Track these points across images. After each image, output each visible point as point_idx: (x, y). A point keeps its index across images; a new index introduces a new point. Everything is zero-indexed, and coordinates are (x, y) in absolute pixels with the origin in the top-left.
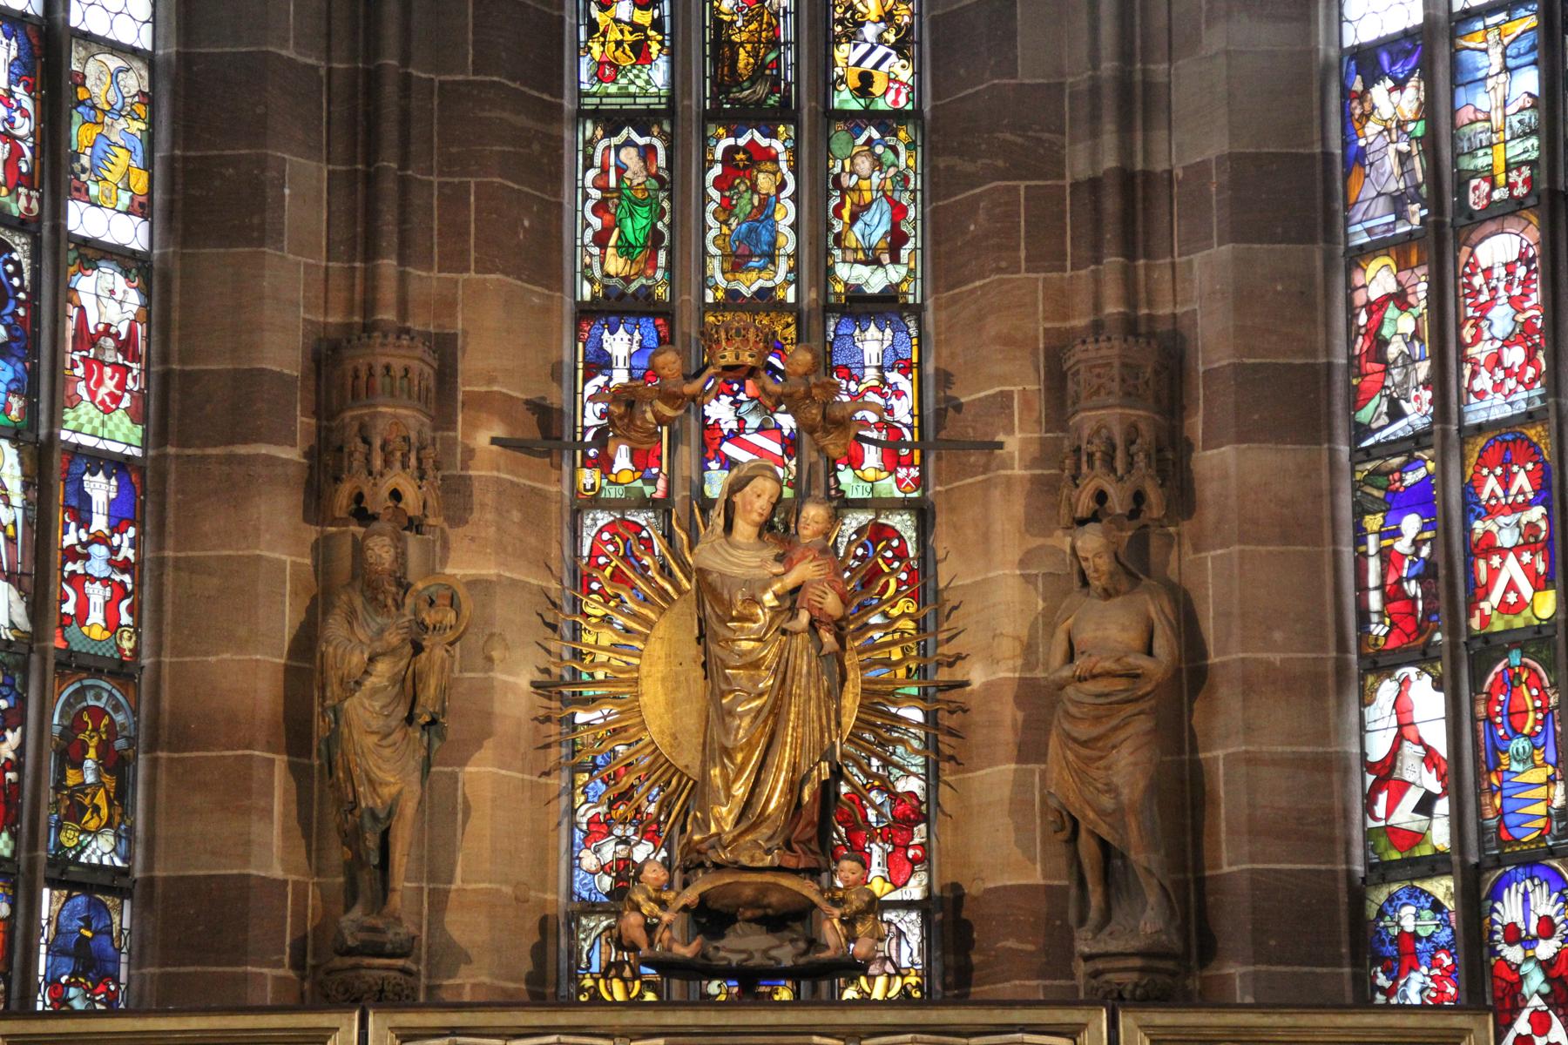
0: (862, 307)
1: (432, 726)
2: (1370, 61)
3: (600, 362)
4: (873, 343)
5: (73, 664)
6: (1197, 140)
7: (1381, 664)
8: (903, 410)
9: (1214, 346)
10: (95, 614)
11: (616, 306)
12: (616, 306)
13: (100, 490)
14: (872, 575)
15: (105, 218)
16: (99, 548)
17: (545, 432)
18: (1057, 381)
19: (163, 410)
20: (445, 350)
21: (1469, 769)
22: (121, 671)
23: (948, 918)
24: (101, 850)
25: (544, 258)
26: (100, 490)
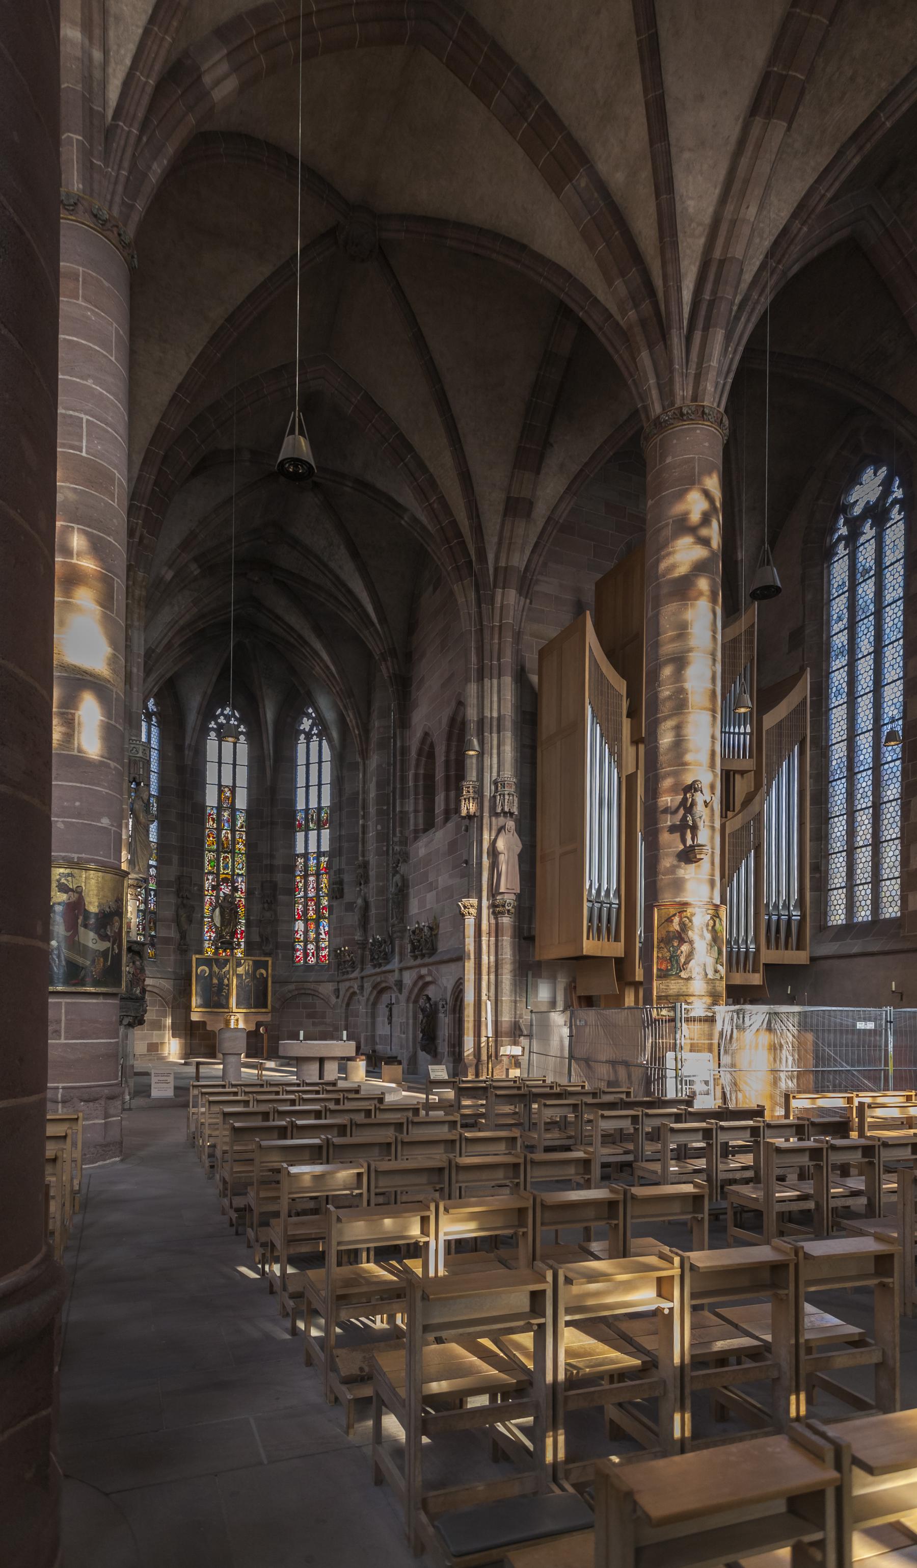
0: (238, 875)
1: (190, 920)
2: (298, 855)
3: (208, 879)
4: (240, 879)
5: (151, 912)
8: (243, 887)
11: (210, 873)
12: (210, 873)
13: (152, 893)
16: (152, 898)
18: (262, 886)
19: (158, 884)
20: (191, 878)
22: (155, 913)
24: (153, 933)
26: (152, 893)
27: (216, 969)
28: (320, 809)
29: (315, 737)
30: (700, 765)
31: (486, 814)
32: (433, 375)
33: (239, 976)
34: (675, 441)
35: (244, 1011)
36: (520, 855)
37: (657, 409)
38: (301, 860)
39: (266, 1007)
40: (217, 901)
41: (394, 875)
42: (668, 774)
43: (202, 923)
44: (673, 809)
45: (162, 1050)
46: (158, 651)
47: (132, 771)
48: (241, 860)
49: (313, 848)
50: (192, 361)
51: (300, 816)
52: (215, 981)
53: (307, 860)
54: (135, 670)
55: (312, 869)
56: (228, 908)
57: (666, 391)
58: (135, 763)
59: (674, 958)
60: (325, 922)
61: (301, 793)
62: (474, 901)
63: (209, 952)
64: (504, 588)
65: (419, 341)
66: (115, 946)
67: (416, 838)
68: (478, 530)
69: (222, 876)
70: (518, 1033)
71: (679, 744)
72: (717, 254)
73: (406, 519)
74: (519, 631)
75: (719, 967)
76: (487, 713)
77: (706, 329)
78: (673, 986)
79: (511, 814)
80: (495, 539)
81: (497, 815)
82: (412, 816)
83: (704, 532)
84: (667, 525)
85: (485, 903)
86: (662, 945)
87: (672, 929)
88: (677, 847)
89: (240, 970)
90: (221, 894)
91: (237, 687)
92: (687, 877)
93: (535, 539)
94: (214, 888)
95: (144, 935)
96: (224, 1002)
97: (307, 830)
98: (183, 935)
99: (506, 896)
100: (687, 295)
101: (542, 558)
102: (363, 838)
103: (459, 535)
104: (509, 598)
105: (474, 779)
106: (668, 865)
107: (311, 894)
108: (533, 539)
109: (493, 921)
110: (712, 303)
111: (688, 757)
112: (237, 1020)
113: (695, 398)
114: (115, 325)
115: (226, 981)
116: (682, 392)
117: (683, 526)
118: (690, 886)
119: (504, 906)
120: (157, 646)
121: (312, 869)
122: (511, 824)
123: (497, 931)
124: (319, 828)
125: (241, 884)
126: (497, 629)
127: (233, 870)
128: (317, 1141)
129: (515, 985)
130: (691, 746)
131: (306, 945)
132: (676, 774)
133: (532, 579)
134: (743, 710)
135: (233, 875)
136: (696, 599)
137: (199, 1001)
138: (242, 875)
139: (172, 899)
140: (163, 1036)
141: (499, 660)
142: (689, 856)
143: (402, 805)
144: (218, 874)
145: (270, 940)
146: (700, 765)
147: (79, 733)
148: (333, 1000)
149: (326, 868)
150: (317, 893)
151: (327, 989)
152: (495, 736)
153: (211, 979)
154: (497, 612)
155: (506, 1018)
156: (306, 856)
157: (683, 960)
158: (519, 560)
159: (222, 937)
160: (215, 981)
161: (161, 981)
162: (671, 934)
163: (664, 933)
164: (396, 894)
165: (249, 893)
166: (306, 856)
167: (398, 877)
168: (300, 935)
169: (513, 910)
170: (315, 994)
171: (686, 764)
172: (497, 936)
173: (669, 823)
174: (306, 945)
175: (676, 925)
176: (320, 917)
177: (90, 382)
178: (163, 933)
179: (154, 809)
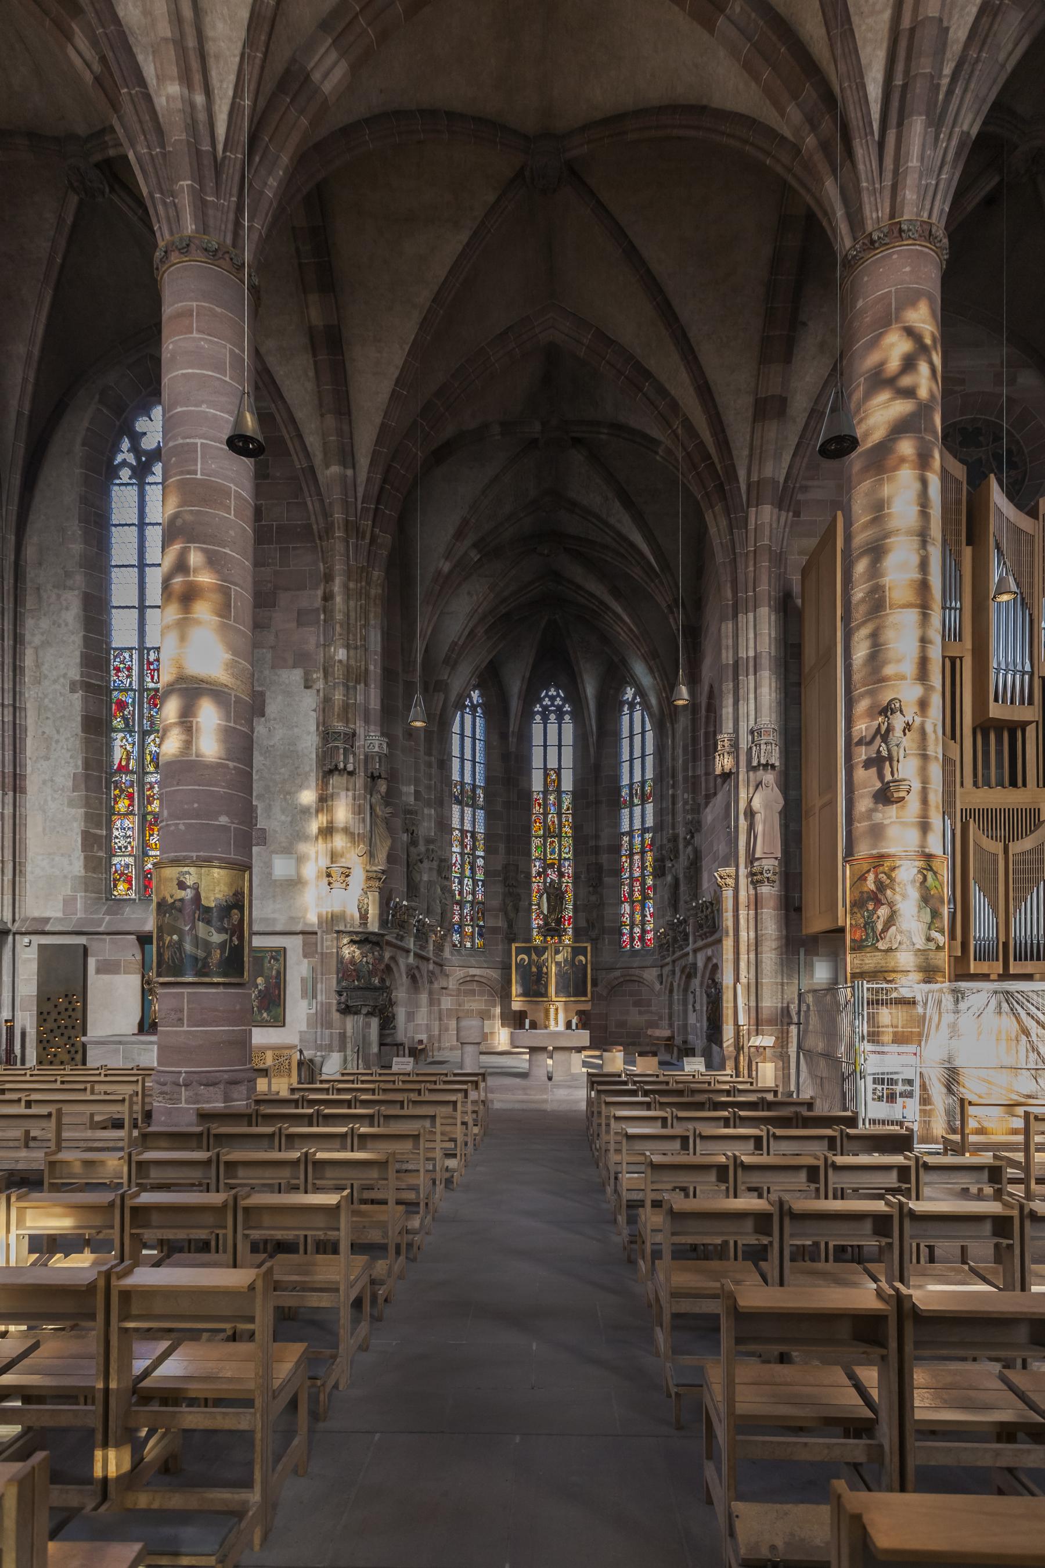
0: (565, 859)
1: (517, 910)
2: (623, 834)
5: (478, 903)
6: (604, 842)
7: (623, 902)
9: (605, 867)
10: (480, 897)
13: (480, 883)
14: (566, 891)
15: (480, 853)
16: (480, 889)
17: (528, 875)
20: (517, 866)
21: (632, 915)
22: (483, 903)
23: (575, 929)
24: (481, 923)
25: (529, 854)
26: (480, 883)
27: (534, 957)
28: (643, 782)
29: (638, 707)
30: (903, 678)
31: (743, 769)
32: (652, 285)
33: (558, 964)
34: (866, 279)
35: (564, 999)
36: (780, 813)
37: (848, 243)
38: (626, 839)
39: (586, 996)
40: (545, 889)
41: (686, 847)
42: (862, 695)
43: (529, 911)
44: (868, 739)
45: (492, 1039)
46: (460, 643)
47: (370, 766)
48: (568, 842)
49: (637, 825)
50: (407, 350)
51: (625, 792)
52: (534, 969)
53: (632, 837)
54: (372, 668)
55: (637, 847)
56: (555, 895)
57: (855, 220)
58: (373, 757)
59: (869, 924)
60: (650, 903)
61: (626, 766)
62: (731, 870)
63: (538, 940)
64: (757, 506)
65: (632, 253)
66: (234, 938)
67: (707, 804)
68: (724, 444)
69: (549, 862)
70: (786, 1020)
71: (876, 657)
72: (906, 23)
73: (660, 452)
74: (781, 552)
75: (934, 934)
76: (742, 654)
77: (900, 124)
78: (870, 961)
79: (773, 766)
80: (746, 452)
81: (755, 769)
82: (703, 779)
83: (906, 381)
84: (859, 385)
85: (743, 871)
86: (855, 910)
87: (866, 889)
88: (874, 786)
89: (559, 958)
90: (549, 880)
91: (554, 665)
92: (886, 822)
93: (796, 440)
94: (539, 874)
95: (472, 926)
96: (543, 991)
97: (632, 805)
98: (510, 926)
99: (764, 862)
100: (874, 90)
101: (806, 460)
102: (673, 809)
103: (709, 457)
104: (765, 516)
105: (731, 731)
106: (863, 809)
107: (637, 874)
108: (793, 440)
109: (752, 892)
110: (905, 87)
111: (889, 670)
112: (557, 1009)
113: (892, 216)
114: (228, 346)
115: (545, 969)
116: (875, 214)
117: (880, 380)
118: (892, 832)
119: (762, 873)
120: (459, 638)
121: (637, 847)
122: (769, 777)
123: (757, 903)
124: (643, 804)
125: (568, 869)
126: (752, 555)
127: (560, 855)
128: (344, 1130)
129: (782, 965)
130: (891, 655)
131: (632, 929)
132: (871, 693)
133: (794, 488)
134: (1005, 598)
135: (560, 860)
136: (896, 468)
137: (520, 990)
138: (568, 859)
139: (499, 889)
140: (493, 1027)
141: (754, 590)
142: (885, 796)
143: (694, 769)
144: (545, 860)
145: (596, 925)
146: (903, 678)
147: (197, 738)
148: (657, 986)
149: (651, 845)
150: (642, 873)
151: (650, 975)
152: (751, 677)
153: (531, 968)
154: (751, 535)
155: (769, 1002)
156: (630, 833)
157: (880, 927)
158: (775, 469)
159: (546, 924)
160: (534, 969)
161: (488, 971)
162: (865, 895)
163: (857, 894)
164: (688, 868)
165: (576, 877)
166: (630, 833)
167: (690, 848)
168: (626, 919)
169: (776, 877)
170: (640, 982)
171: (884, 680)
172: (756, 909)
173: (864, 757)
174: (632, 929)
175: (870, 884)
176: (645, 897)
177: (204, 408)
178: (491, 923)
179: (481, 801)
